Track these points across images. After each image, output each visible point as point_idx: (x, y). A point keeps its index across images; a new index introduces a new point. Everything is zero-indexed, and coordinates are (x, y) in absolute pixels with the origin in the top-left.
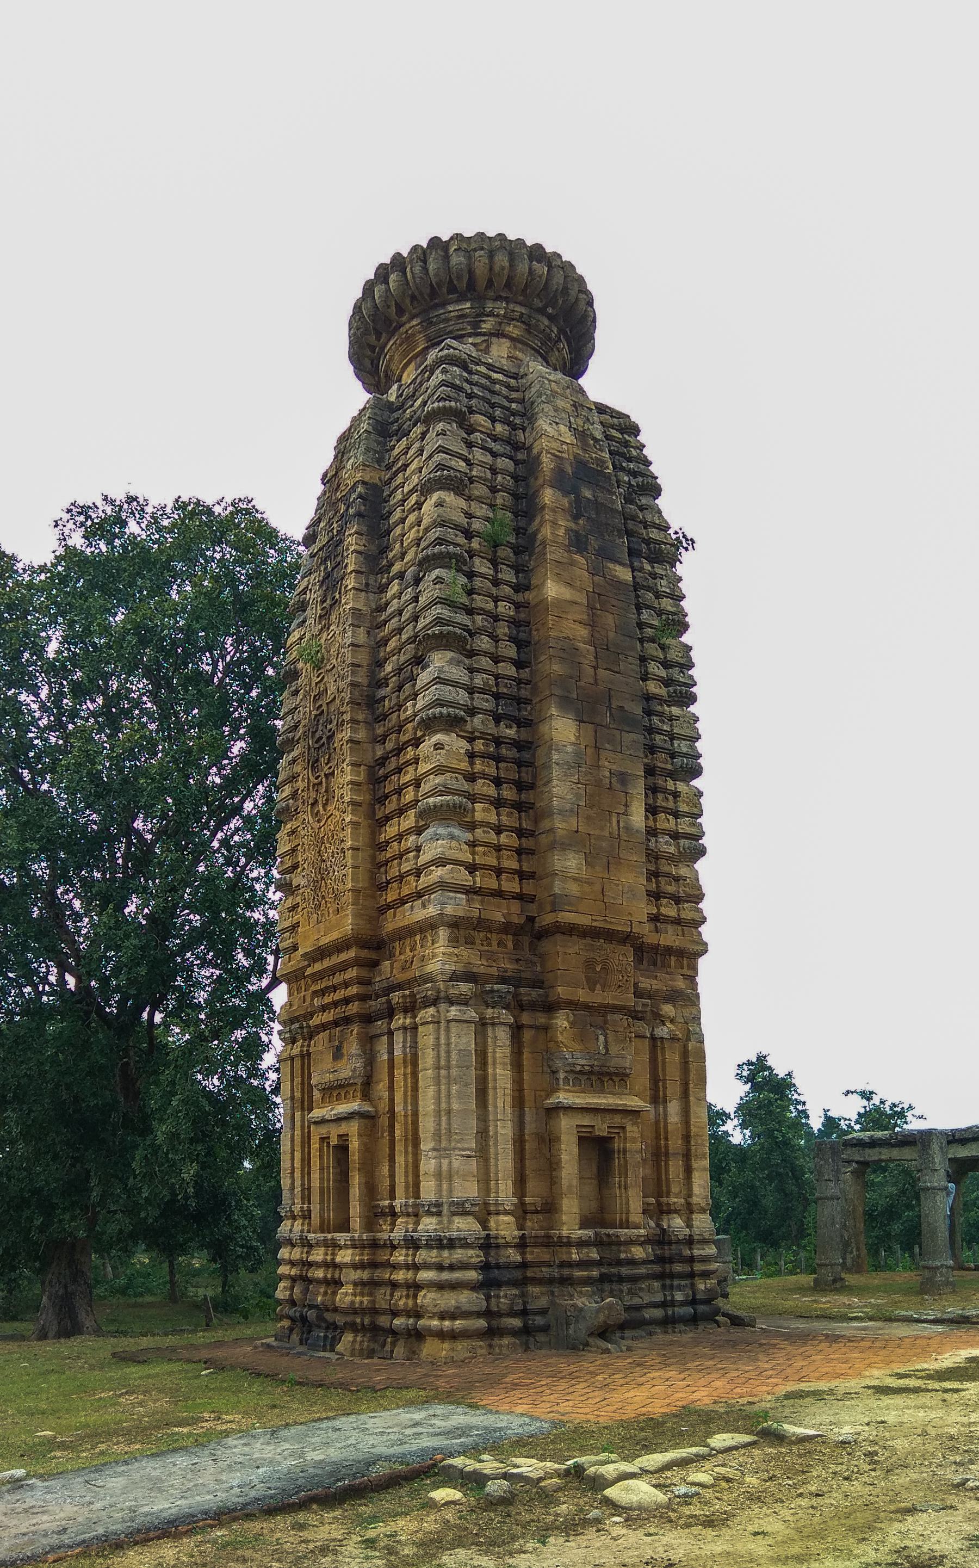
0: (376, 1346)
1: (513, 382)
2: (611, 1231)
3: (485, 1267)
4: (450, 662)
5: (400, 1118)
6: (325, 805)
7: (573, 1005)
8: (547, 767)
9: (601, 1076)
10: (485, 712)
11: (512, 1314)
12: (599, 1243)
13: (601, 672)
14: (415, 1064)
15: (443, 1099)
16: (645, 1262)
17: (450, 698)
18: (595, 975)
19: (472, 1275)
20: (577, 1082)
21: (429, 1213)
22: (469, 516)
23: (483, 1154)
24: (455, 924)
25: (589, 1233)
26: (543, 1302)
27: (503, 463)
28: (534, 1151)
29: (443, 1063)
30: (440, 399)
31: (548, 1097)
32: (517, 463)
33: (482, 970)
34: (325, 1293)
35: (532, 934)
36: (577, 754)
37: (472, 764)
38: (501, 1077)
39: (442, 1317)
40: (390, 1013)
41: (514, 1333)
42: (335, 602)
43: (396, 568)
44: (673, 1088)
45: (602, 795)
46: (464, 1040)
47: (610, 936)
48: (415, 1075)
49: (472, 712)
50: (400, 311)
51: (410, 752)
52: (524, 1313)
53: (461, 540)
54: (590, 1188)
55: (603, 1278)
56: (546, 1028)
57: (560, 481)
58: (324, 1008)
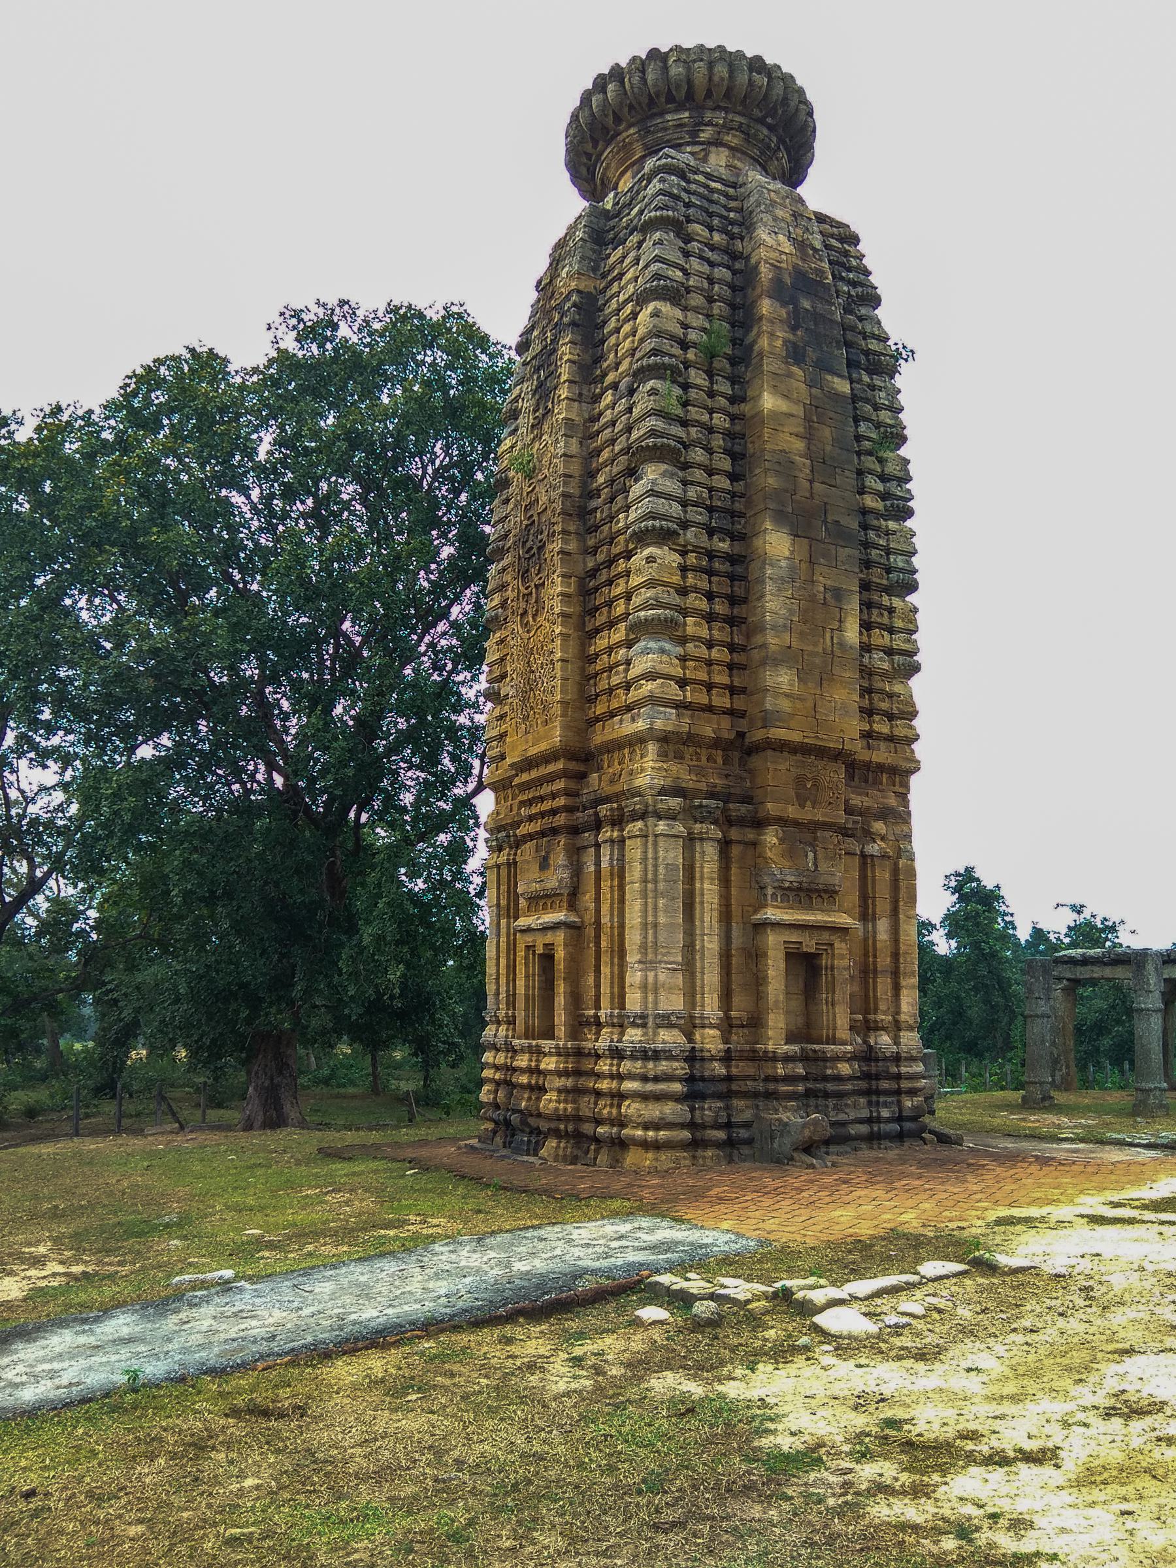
0: (580, 1153)
1: (731, 191)
2: (816, 1047)
3: (690, 1079)
4: (663, 475)
5: (606, 929)
6: (534, 616)
7: (782, 821)
8: (761, 581)
9: (809, 893)
10: (698, 525)
11: (717, 1126)
12: (804, 1058)
13: (816, 485)
14: (622, 877)
15: (650, 913)
16: (851, 1078)
17: (662, 511)
18: (805, 792)
19: (677, 1087)
20: (785, 898)
21: (634, 1025)
22: (685, 326)
23: (689, 967)
24: (664, 739)
25: (794, 1048)
26: (748, 1115)
27: (721, 273)
28: (741, 966)
29: (650, 876)
30: (657, 209)
31: (755, 912)
32: (734, 272)
33: (691, 785)
34: (530, 1099)
35: (741, 749)
36: (792, 569)
37: (684, 577)
38: (709, 892)
39: (646, 1128)
40: (598, 825)
41: (718, 1145)
42: (548, 412)
43: (610, 378)
44: (883, 907)
45: (816, 611)
46: (671, 855)
47: (821, 752)
48: (622, 887)
49: (685, 525)
50: (618, 119)
51: (622, 565)
52: (728, 1125)
53: (676, 350)
54: (797, 1004)
55: (808, 1093)
56: (754, 844)
57: (778, 291)
58: (531, 818)
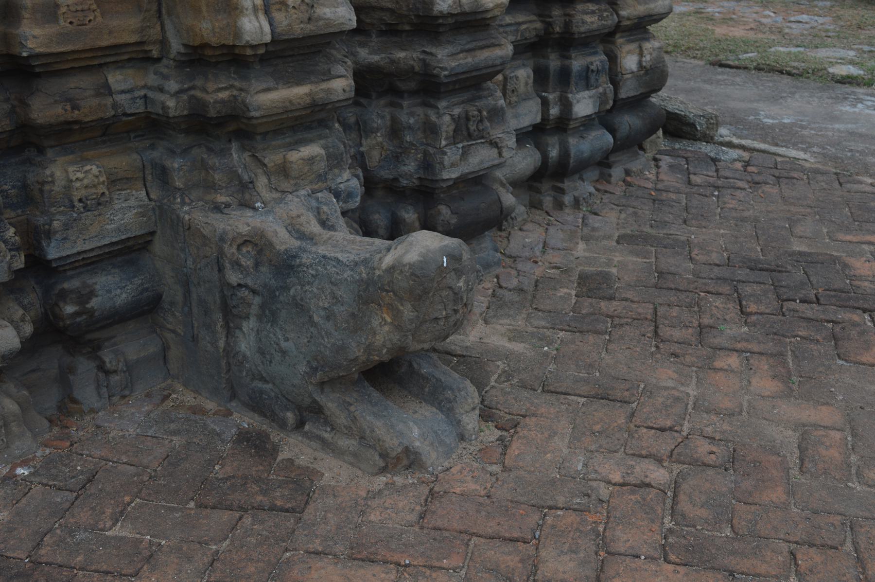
26: (124, 216)
